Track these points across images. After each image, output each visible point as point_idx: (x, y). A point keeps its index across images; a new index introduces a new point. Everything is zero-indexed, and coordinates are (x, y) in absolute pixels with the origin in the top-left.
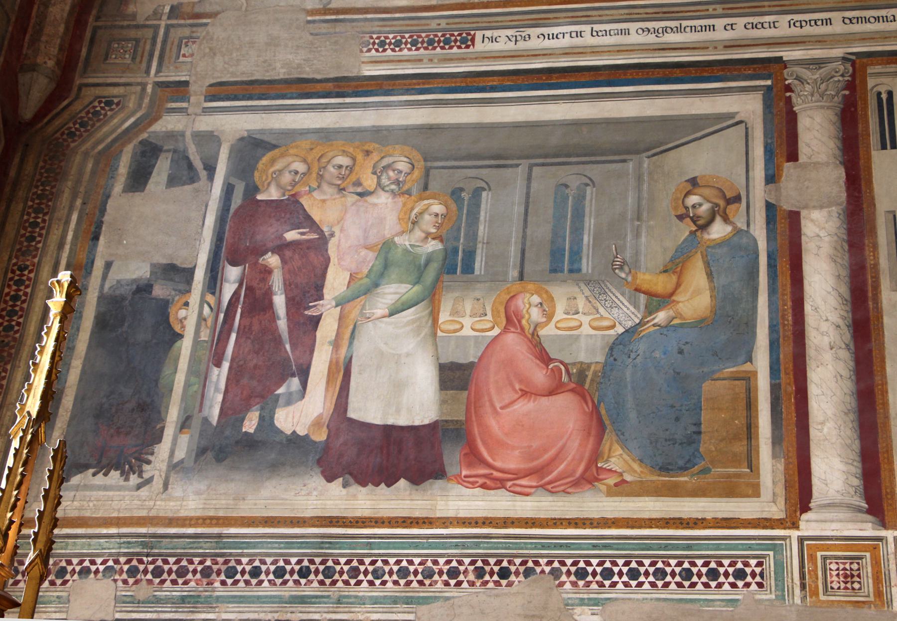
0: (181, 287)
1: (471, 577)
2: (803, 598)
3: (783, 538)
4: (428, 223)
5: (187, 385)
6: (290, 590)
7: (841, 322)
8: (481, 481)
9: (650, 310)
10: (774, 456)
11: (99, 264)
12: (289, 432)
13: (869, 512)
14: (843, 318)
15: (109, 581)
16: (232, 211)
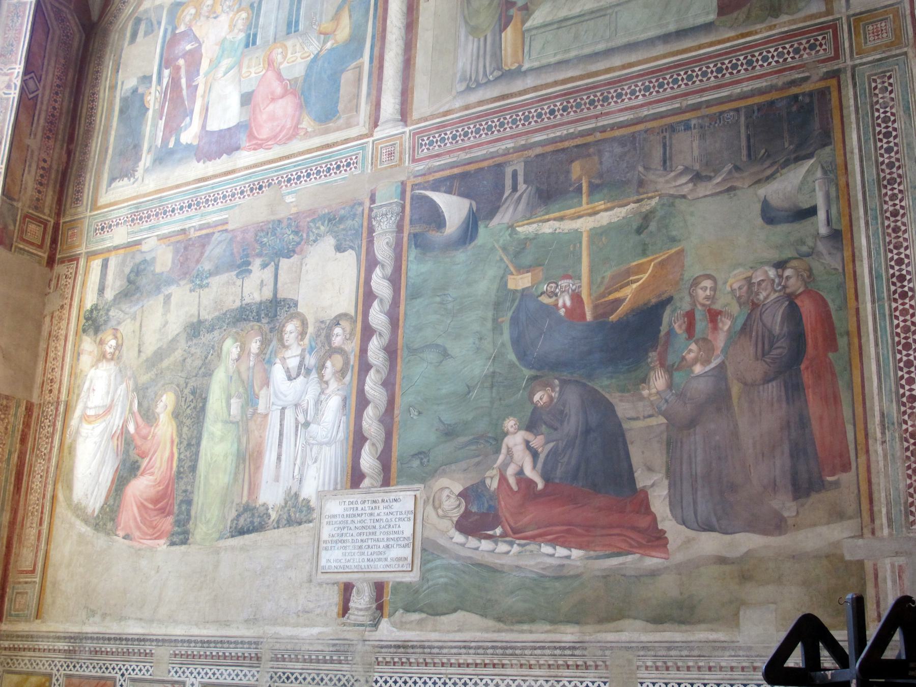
0: (148, 85)
1: (249, 192)
2: (372, 170)
3: (366, 143)
4: (240, 24)
5: (151, 131)
6: (186, 215)
7: (402, 28)
8: (253, 147)
9: (325, 42)
10: (367, 103)
11: (119, 83)
12: (185, 143)
13: (401, 120)
14: (402, 23)
15: (125, 226)
16: (167, 40)
